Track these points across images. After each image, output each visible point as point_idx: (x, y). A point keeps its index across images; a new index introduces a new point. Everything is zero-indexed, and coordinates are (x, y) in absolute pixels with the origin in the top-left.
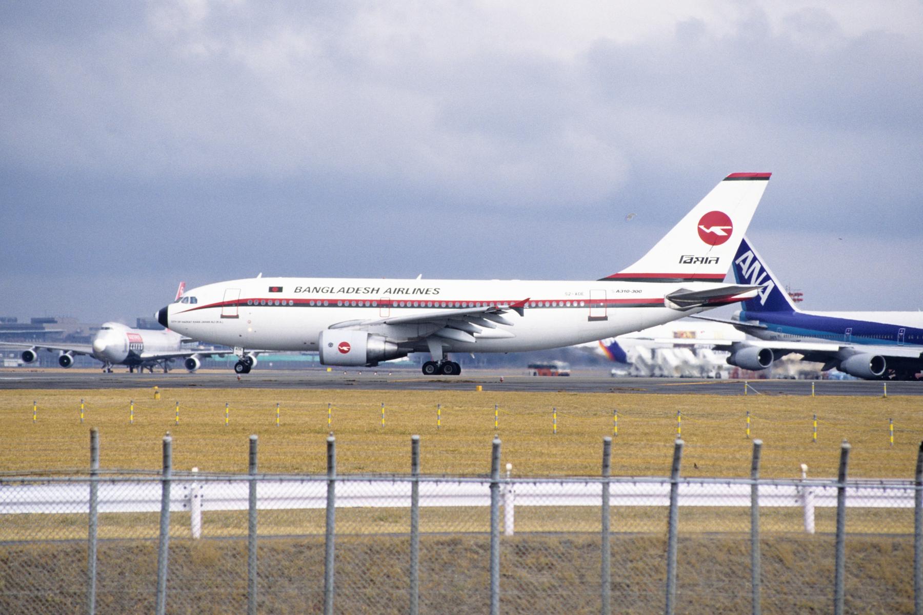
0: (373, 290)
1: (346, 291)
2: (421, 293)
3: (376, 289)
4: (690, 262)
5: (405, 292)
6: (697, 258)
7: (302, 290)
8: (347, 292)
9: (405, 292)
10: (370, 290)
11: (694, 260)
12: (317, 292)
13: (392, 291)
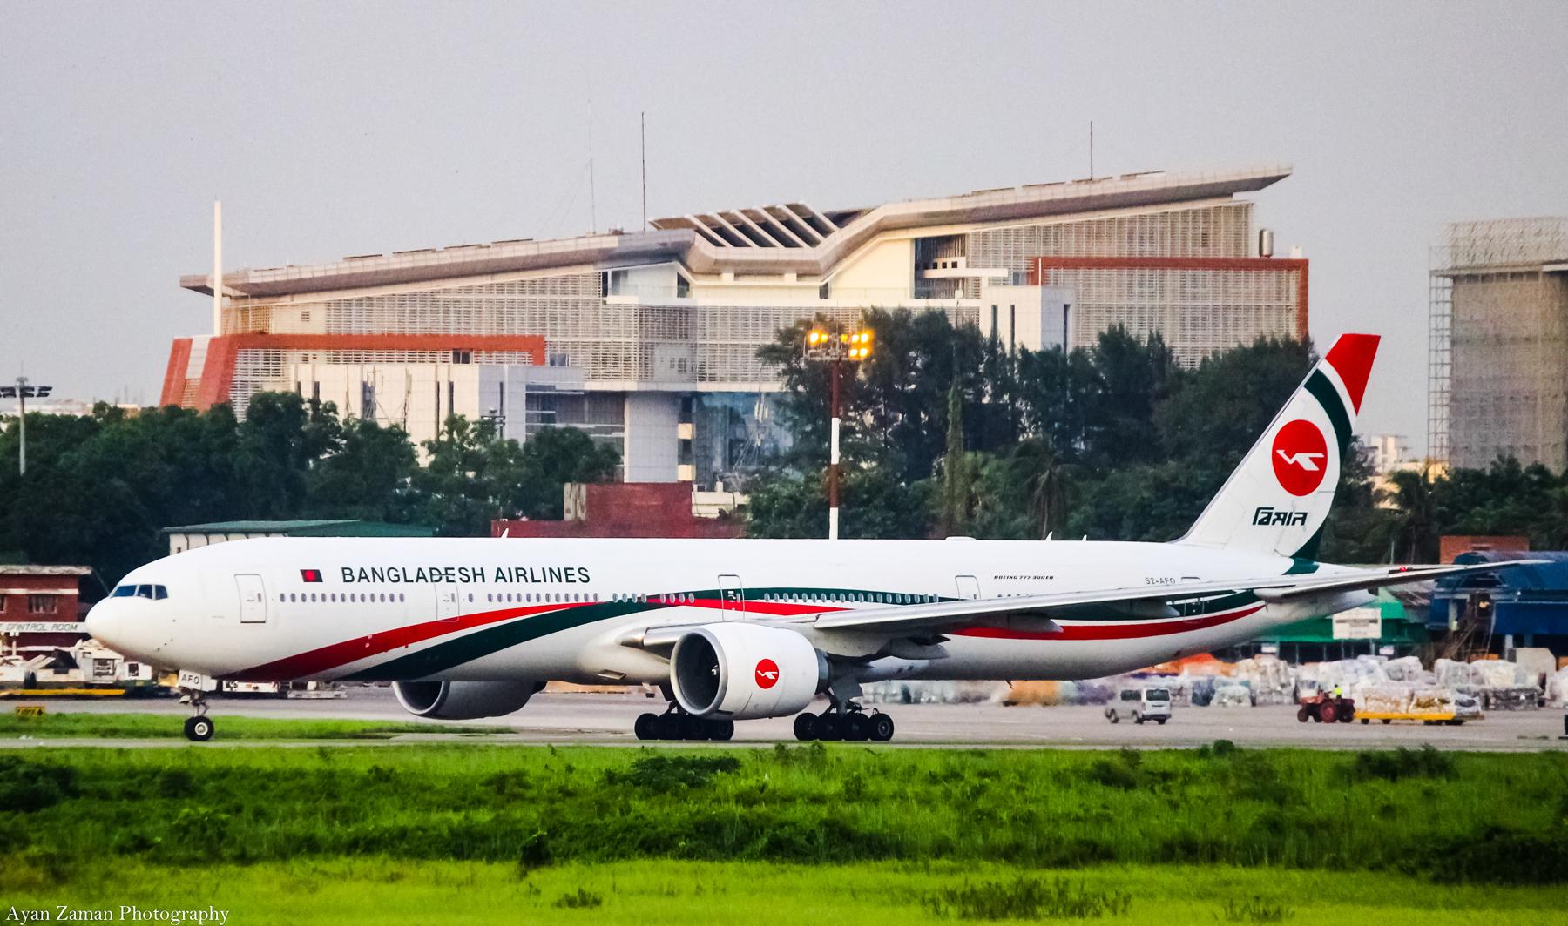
0: (475, 575)
2: (560, 580)
4: (1267, 523)
5: (529, 576)
9: (529, 576)
12: (382, 580)
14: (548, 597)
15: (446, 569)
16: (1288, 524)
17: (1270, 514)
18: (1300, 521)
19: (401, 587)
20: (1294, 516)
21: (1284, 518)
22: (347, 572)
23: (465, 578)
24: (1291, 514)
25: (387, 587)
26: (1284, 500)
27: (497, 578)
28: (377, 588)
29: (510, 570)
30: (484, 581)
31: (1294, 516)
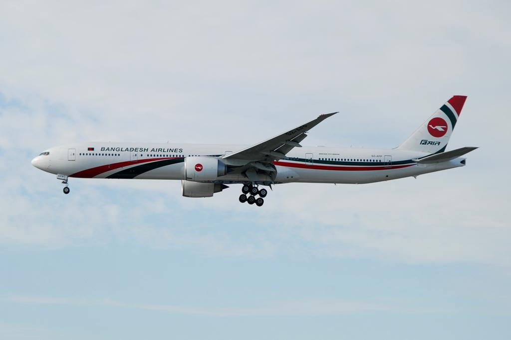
0: (145, 149)
1: (129, 150)
3: (146, 149)
5: (162, 151)
6: (429, 142)
7: (105, 149)
9: (162, 151)
10: (143, 150)
14: (167, 156)
19: (120, 152)
21: (431, 143)
25: (115, 152)
28: (112, 152)
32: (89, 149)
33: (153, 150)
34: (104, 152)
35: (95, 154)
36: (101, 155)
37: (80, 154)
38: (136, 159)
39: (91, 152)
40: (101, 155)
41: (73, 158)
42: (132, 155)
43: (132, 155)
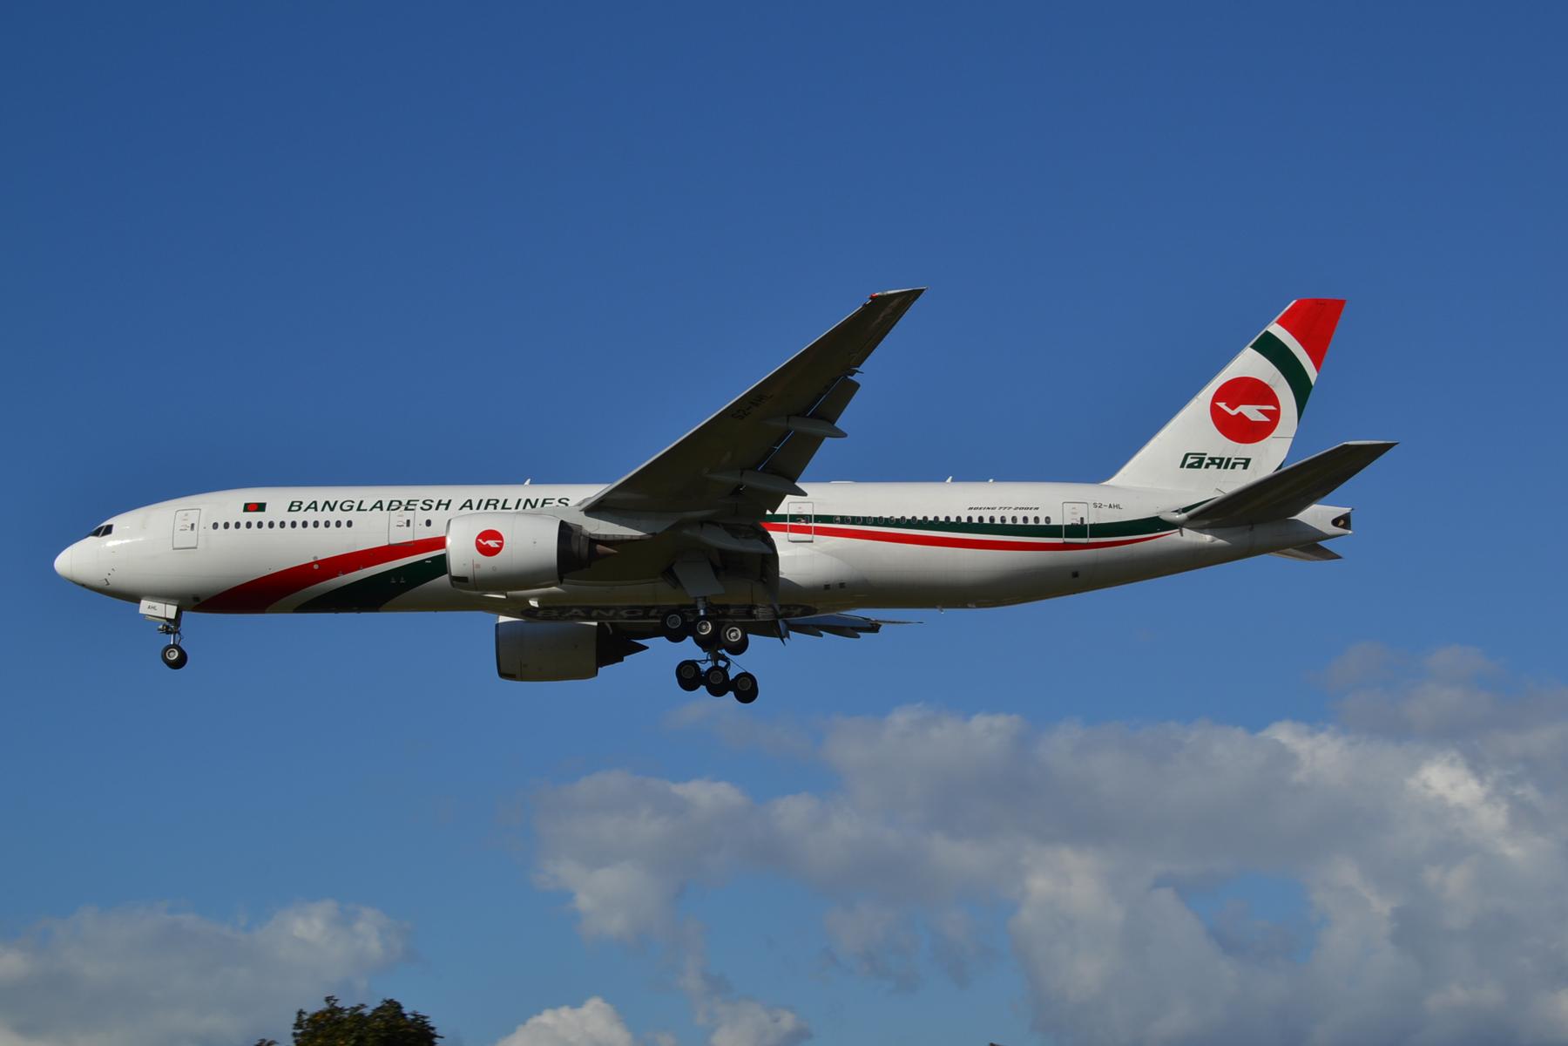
0: (440, 503)
1: (385, 507)
4: (1199, 467)
5: (500, 505)
6: (1210, 459)
7: (304, 507)
8: (388, 509)
9: (500, 505)
10: (434, 505)
11: (1207, 461)
12: (332, 509)
13: (475, 506)
15: (409, 501)
16: (1226, 467)
17: (1203, 459)
18: (1242, 466)
19: (353, 515)
20: (1233, 461)
21: (1220, 463)
22: (295, 504)
23: (428, 507)
24: (1229, 460)
25: (337, 515)
26: (1221, 445)
27: (464, 506)
29: (481, 501)
30: (447, 509)
31: (1233, 461)
32: (248, 508)
33: (469, 504)
34: (299, 517)
35: (266, 525)
36: (288, 525)
37: (215, 526)
38: (410, 539)
39: (254, 517)
40: (288, 525)
41: (188, 538)
42: (394, 522)
43: (394, 522)
